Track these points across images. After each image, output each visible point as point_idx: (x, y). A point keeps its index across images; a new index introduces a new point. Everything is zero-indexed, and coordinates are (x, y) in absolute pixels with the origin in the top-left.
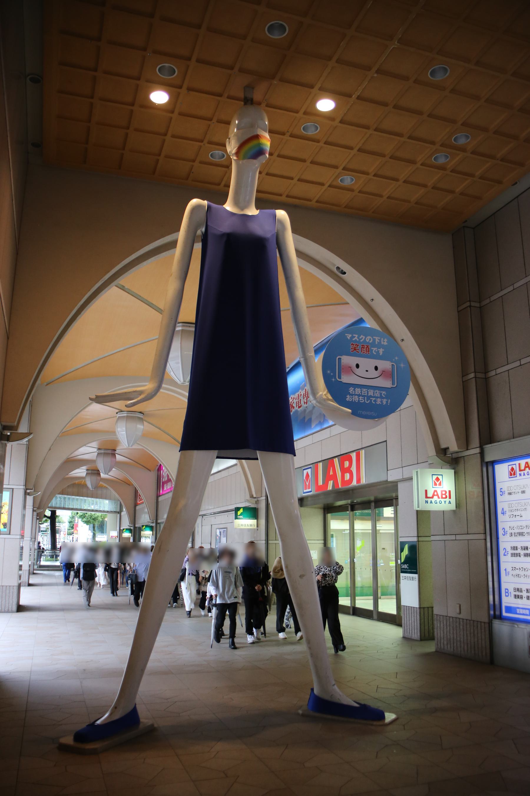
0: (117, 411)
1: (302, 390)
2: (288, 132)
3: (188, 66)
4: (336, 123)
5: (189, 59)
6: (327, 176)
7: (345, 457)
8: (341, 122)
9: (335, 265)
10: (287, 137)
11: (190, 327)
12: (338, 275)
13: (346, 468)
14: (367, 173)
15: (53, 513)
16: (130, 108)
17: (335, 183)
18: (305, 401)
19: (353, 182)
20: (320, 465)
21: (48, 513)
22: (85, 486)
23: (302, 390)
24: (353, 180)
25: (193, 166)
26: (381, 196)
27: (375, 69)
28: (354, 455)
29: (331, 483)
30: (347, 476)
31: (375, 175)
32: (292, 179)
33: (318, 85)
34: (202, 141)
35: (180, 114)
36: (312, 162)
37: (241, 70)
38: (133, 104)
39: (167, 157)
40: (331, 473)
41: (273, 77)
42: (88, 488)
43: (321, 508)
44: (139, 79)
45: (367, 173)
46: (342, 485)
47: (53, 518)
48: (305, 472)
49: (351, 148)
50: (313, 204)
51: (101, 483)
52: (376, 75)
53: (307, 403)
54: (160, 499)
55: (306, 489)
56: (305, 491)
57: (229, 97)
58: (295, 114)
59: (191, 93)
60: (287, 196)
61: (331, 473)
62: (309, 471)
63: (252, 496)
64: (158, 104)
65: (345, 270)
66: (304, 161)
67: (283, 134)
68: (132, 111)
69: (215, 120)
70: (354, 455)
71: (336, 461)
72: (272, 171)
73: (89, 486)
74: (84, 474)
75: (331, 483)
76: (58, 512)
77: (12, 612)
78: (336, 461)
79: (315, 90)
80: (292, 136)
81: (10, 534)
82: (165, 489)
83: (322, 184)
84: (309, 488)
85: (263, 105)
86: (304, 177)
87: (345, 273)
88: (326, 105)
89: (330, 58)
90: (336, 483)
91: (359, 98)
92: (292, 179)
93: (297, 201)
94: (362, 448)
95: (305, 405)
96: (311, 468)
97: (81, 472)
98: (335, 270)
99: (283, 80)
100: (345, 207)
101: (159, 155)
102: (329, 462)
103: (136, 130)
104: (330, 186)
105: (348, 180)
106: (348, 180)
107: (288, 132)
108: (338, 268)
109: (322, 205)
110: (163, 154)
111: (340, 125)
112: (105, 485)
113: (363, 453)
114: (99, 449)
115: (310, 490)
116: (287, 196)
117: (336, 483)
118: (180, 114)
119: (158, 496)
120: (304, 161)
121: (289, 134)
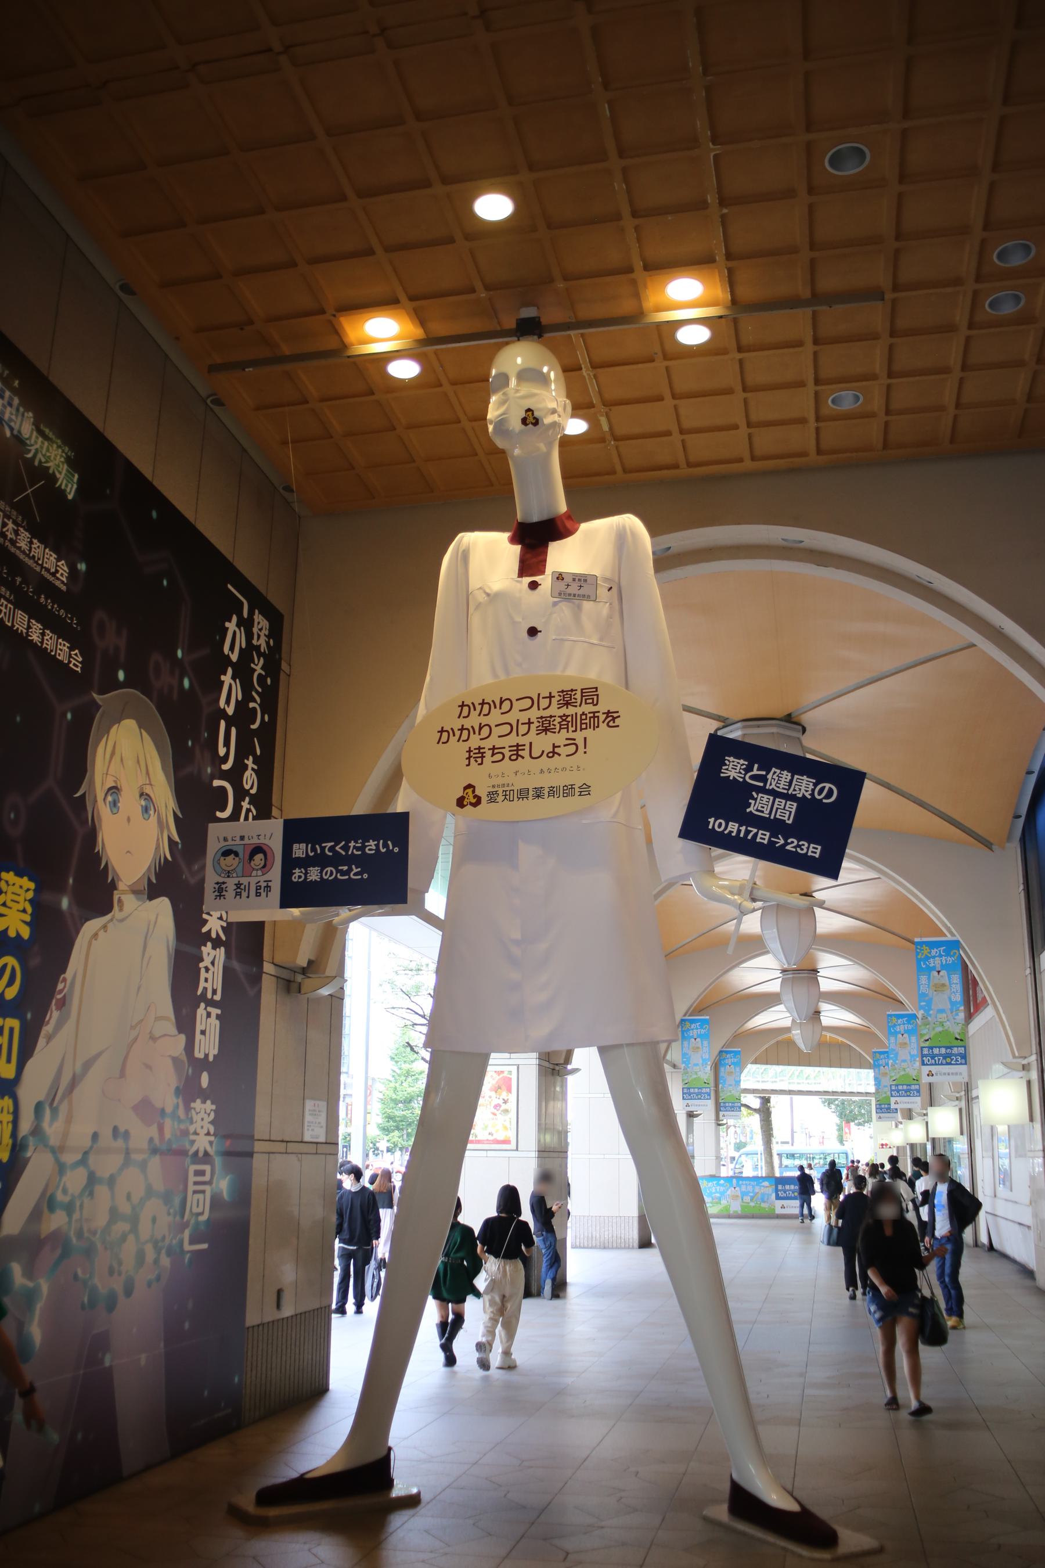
10: (660, 364)
15: (766, 1101)
21: (756, 1103)
22: (791, 1043)
24: (857, 398)
32: (736, 427)
47: (765, 1112)
49: (800, 344)
52: (725, 211)
63: (1014, 1057)
73: (802, 1046)
74: (787, 1023)
79: (639, 273)
81: (517, 1149)
91: (729, 256)
92: (736, 427)
100: (885, 446)
103: (410, 427)
105: (847, 400)
106: (847, 400)
114: (784, 971)
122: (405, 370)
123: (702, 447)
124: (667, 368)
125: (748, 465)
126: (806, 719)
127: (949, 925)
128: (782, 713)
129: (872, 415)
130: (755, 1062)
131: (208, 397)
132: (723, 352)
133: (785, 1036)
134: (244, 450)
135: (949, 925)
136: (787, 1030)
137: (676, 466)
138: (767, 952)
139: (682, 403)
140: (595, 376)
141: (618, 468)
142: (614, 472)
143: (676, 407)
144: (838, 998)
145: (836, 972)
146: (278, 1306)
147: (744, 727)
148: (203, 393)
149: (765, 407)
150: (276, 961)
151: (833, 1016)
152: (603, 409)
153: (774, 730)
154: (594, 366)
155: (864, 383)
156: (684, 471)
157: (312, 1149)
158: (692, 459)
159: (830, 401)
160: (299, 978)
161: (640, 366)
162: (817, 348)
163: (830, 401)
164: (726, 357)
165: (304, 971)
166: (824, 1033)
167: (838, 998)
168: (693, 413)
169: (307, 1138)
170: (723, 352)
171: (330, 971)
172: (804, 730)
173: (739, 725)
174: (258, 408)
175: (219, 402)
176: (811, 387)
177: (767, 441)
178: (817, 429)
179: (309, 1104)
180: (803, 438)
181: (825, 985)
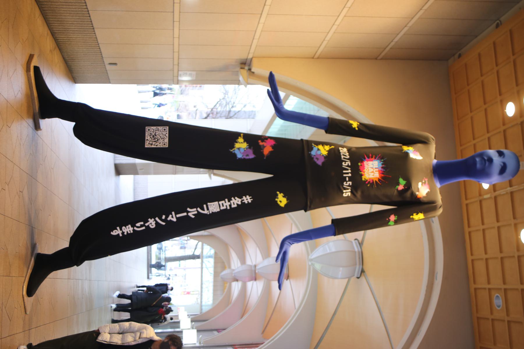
6: (496, 282)
10: (513, 222)
11: (359, 258)
15: (198, 257)
21: (197, 253)
22: (224, 268)
24: (499, 307)
42: (222, 272)
47: (194, 257)
50: (473, 286)
51: (228, 285)
66: (501, 251)
67: (514, 218)
72: (487, 232)
74: (233, 267)
76: (199, 261)
77: (114, 160)
80: (516, 225)
83: (489, 282)
86: (490, 262)
97: (235, 264)
100: (478, 318)
106: (498, 302)
109: (474, 294)
112: (226, 290)
114: (255, 266)
116: (473, 260)
123: (477, 238)
124: (510, 225)
125: (470, 258)
126: (363, 278)
127: (275, 340)
128: (365, 269)
129: (492, 313)
130: (216, 253)
131: (500, 21)
132: (518, 250)
133: (227, 266)
134: (476, 36)
135: (275, 340)
136: (230, 267)
137: (469, 227)
138: (263, 259)
139: (495, 231)
140: (507, 193)
141: (468, 202)
142: (466, 199)
143: (494, 228)
144: (244, 289)
145: (255, 289)
146: (110, 64)
147: (359, 252)
148: (502, 19)
149: (495, 266)
150: (254, 59)
151: (236, 287)
152: (493, 196)
154: (512, 193)
155: (505, 310)
156: (467, 230)
157: (176, 74)
158: (473, 234)
159: (498, 295)
160: (247, 68)
162: (520, 290)
163: (498, 295)
164: (516, 250)
165: (250, 70)
166: (228, 283)
167: (244, 289)
168: (492, 235)
169: (180, 73)
170: (518, 250)
171: (250, 80)
172: (358, 278)
173: (360, 250)
174: (494, 44)
175: (497, 26)
177: (480, 267)
178: (485, 289)
179: (194, 73)
180: (481, 282)
181: (250, 284)
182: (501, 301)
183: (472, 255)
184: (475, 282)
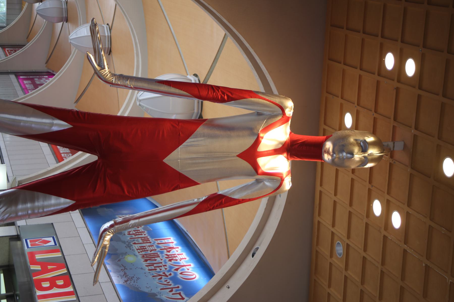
0: (110, 25)
1: (143, 228)
2: (372, 187)
3: (414, 87)
4: (384, 233)
5: (420, 88)
6: (341, 230)
7: (68, 279)
8: (385, 237)
9: (260, 245)
12: (250, 250)
13: (56, 283)
14: (346, 269)
16: (380, 35)
17: (336, 238)
18: (131, 233)
19: (338, 256)
20: (59, 255)
23: (143, 228)
24: (340, 255)
25: (338, 97)
26: (329, 286)
27: (428, 263)
28: (70, 289)
29: (38, 268)
30: (46, 285)
31: (346, 277)
32: (335, 194)
33: (411, 211)
34: (358, 105)
35: (378, 82)
36: (350, 213)
37: (415, 137)
38: (383, 37)
39: (344, 71)
40: (50, 267)
41: (412, 168)
43: (9, 261)
44: (402, 41)
45: (346, 269)
46: (35, 280)
48: (51, 239)
49: (365, 250)
50: (317, 219)
52: (424, 265)
53: (129, 234)
54: (13, 77)
55: (30, 241)
56: (28, 241)
57: (394, 127)
58: (386, 192)
59: (395, 91)
60: (321, 192)
61: (50, 267)
62: (52, 243)
64: (384, 60)
65: (255, 256)
66: (351, 205)
67: (370, 182)
68: (377, 36)
69: (376, 115)
70: (70, 289)
71: (64, 271)
75: (38, 268)
78: (64, 271)
80: (370, 190)
82: (25, 82)
83: (333, 226)
84: (31, 245)
85: (391, 161)
86: (338, 207)
87: (253, 256)
88: (396, 220)
89: (432, 219)
90: (38, 273)
91: (405, 251)
92: (335, 194)
93: (317, 202)
94: (78, 297)
95: (126, 233)
96: (56, 244)
98: (256, 246)
99: (411, 176)
101: (345, 64)
102: (63, 263)
103: (363, 40)
104: (333, 233)
105: (340, 249)
106: (340, 249)
107: (372, 187)
108: (257, 249)
109: (316, 226)
110: (346, 67)
111: (382, 236)
112: (25, 7)
113: (74, 298)
115: (30, 246)
116: (321, 192)
117: (38, 273)
118: (378, 82)
119: (17, 74)
120: (351, 205)
121: (371, 188)
122: (390, 61)
125: (318, 188)
129: (331, 256)
153: (196, 111)
161: (368, 176)
176: (347, 241)
180: (326, 219)
182: (342, 248)
183: (321, 185)
184: (319, 215)
